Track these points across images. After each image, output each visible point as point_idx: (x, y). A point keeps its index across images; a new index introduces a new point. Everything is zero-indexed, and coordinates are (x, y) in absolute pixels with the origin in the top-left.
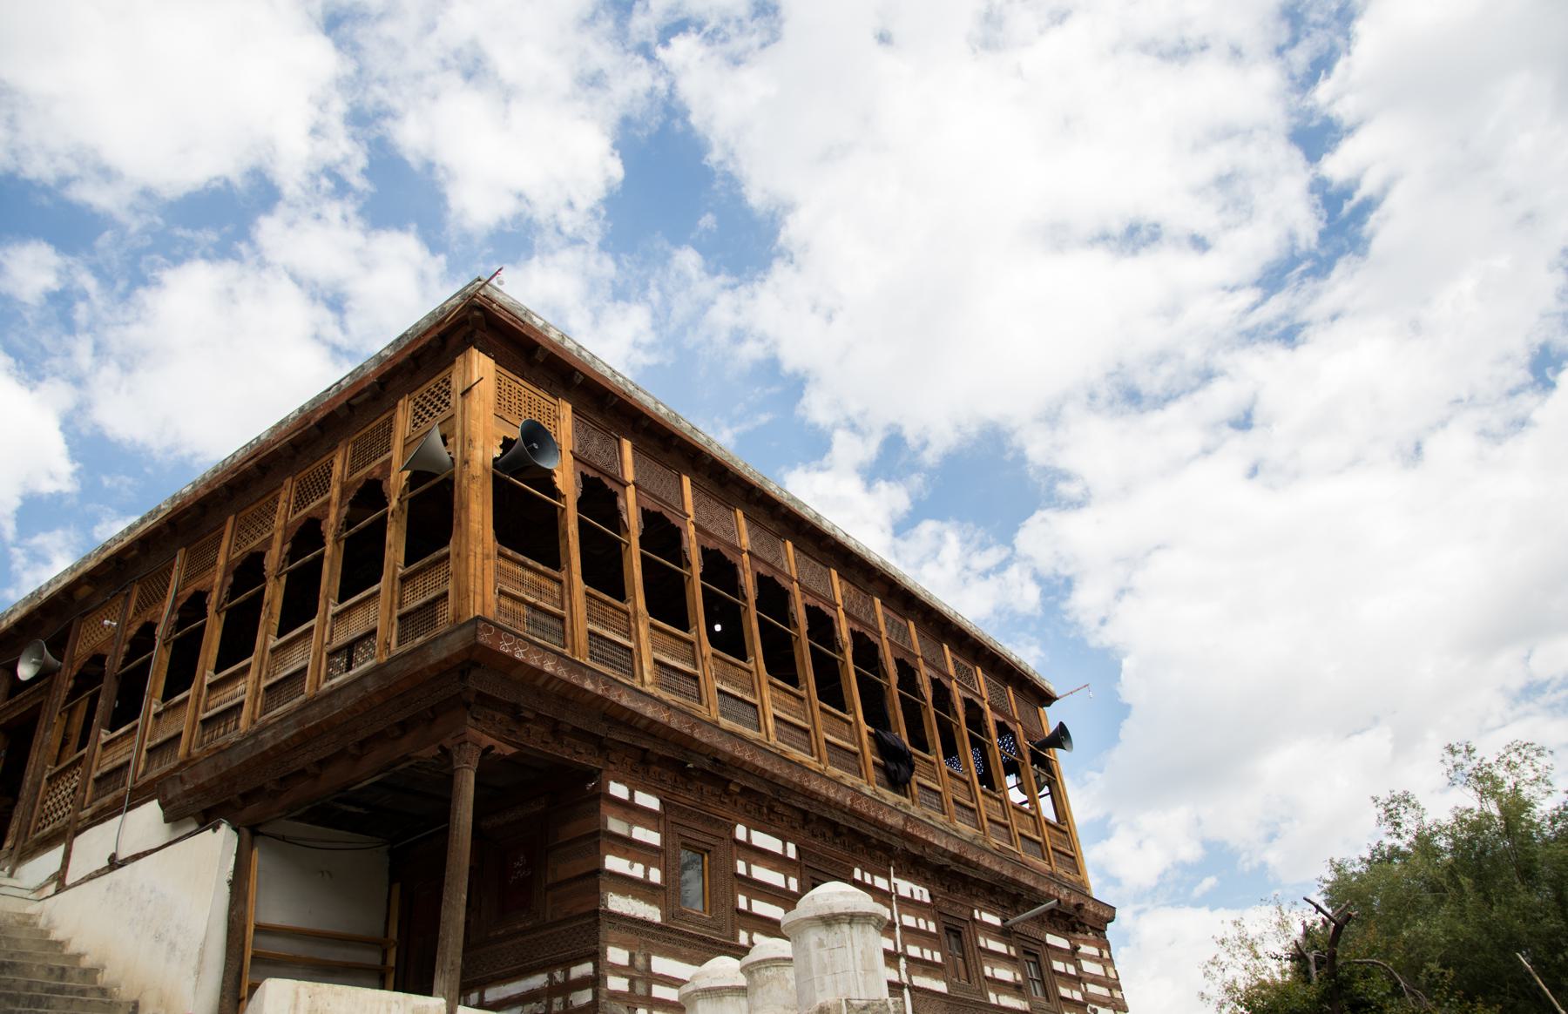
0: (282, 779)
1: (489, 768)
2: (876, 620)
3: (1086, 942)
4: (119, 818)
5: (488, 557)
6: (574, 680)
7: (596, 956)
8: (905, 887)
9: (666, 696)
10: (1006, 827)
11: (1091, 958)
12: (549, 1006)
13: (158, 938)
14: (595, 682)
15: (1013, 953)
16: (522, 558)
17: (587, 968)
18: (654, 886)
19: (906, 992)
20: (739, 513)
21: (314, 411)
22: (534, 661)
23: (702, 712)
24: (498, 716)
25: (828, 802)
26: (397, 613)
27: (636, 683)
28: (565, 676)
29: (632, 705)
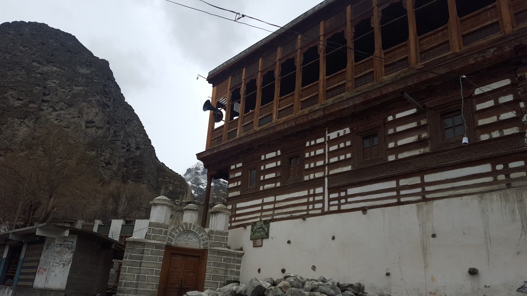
8: (333, 135)
19: (326, 179)
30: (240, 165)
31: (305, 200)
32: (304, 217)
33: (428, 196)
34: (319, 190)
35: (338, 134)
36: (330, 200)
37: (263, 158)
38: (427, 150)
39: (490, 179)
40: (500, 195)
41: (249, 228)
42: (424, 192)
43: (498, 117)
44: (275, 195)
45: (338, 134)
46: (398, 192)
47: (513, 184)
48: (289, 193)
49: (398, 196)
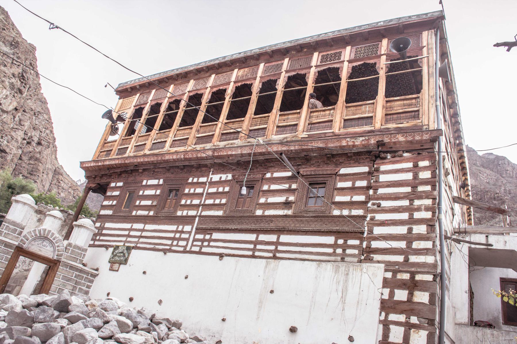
8: (216, 178)
14: (101, 162)
19: (197, 219)
22: (89, 165)
30: (120, 184)
31: (172, 235)
32: (165, 251)
33: (278, 255)
34: (187, 228)
36: (195, 240)
37: (144, 183)
38: (290, 212)
39: (330, 250)
40: (333, 265)
41: (111, 250)
42: (276, 251)
43: (352, 197)
44: (145, 223)
45: (221, 178)
46: (255, 246)
47: (347, 259)
48: (159, 224)
49: (254, 250)
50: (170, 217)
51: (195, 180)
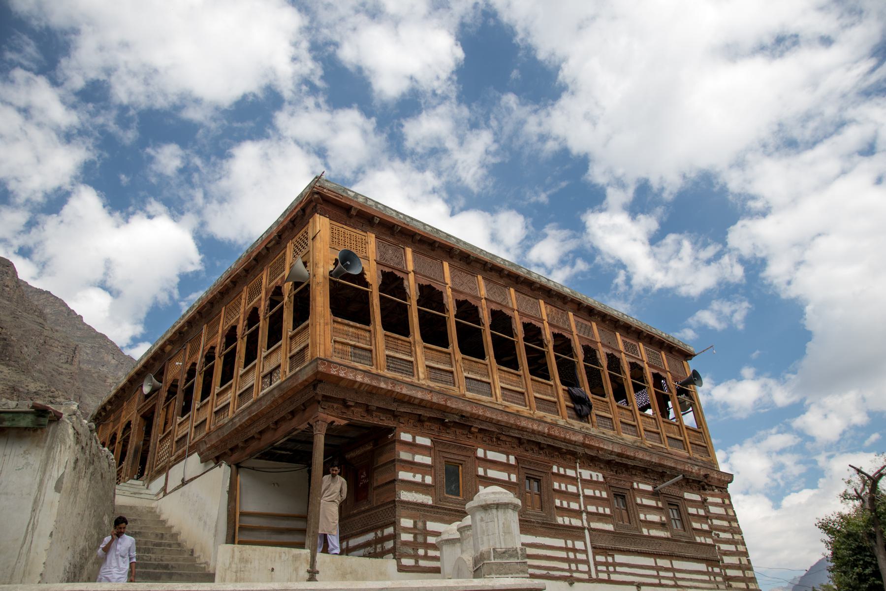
0: (246, 441)
1: (332, 432)
2: (569, 325)
3: (712, 496)
4: (182, 463)
5: (327, 324)
6: (374, 383)
7: (394, 524)
8: (586, 474)
9: (432, 384)
10: (658, 434)
11: (716, 505)
12: (375, 549)
13: (200, 519)
14: (386, 383)
15: (660, 505)
16: (346, 321)
17: (390, 530)
18: (428, 486)
19: (586, 532)
20: (480, 277)
21: (252, 252)
22: (351, 376)
23: (455, 391)
24: (335, 406)
25: (533, 432)
26: (289, 355)
27: (415, 380)
28: (369, 382)
29: (409, 393)
31: (563, 554)
32: (571, 581)
34: (579, 545)
35: (591, 476)
39: (706, 578)
42: (674, 578)
48: (536, 534)
50: (549, 524)
51: (562, 471)
